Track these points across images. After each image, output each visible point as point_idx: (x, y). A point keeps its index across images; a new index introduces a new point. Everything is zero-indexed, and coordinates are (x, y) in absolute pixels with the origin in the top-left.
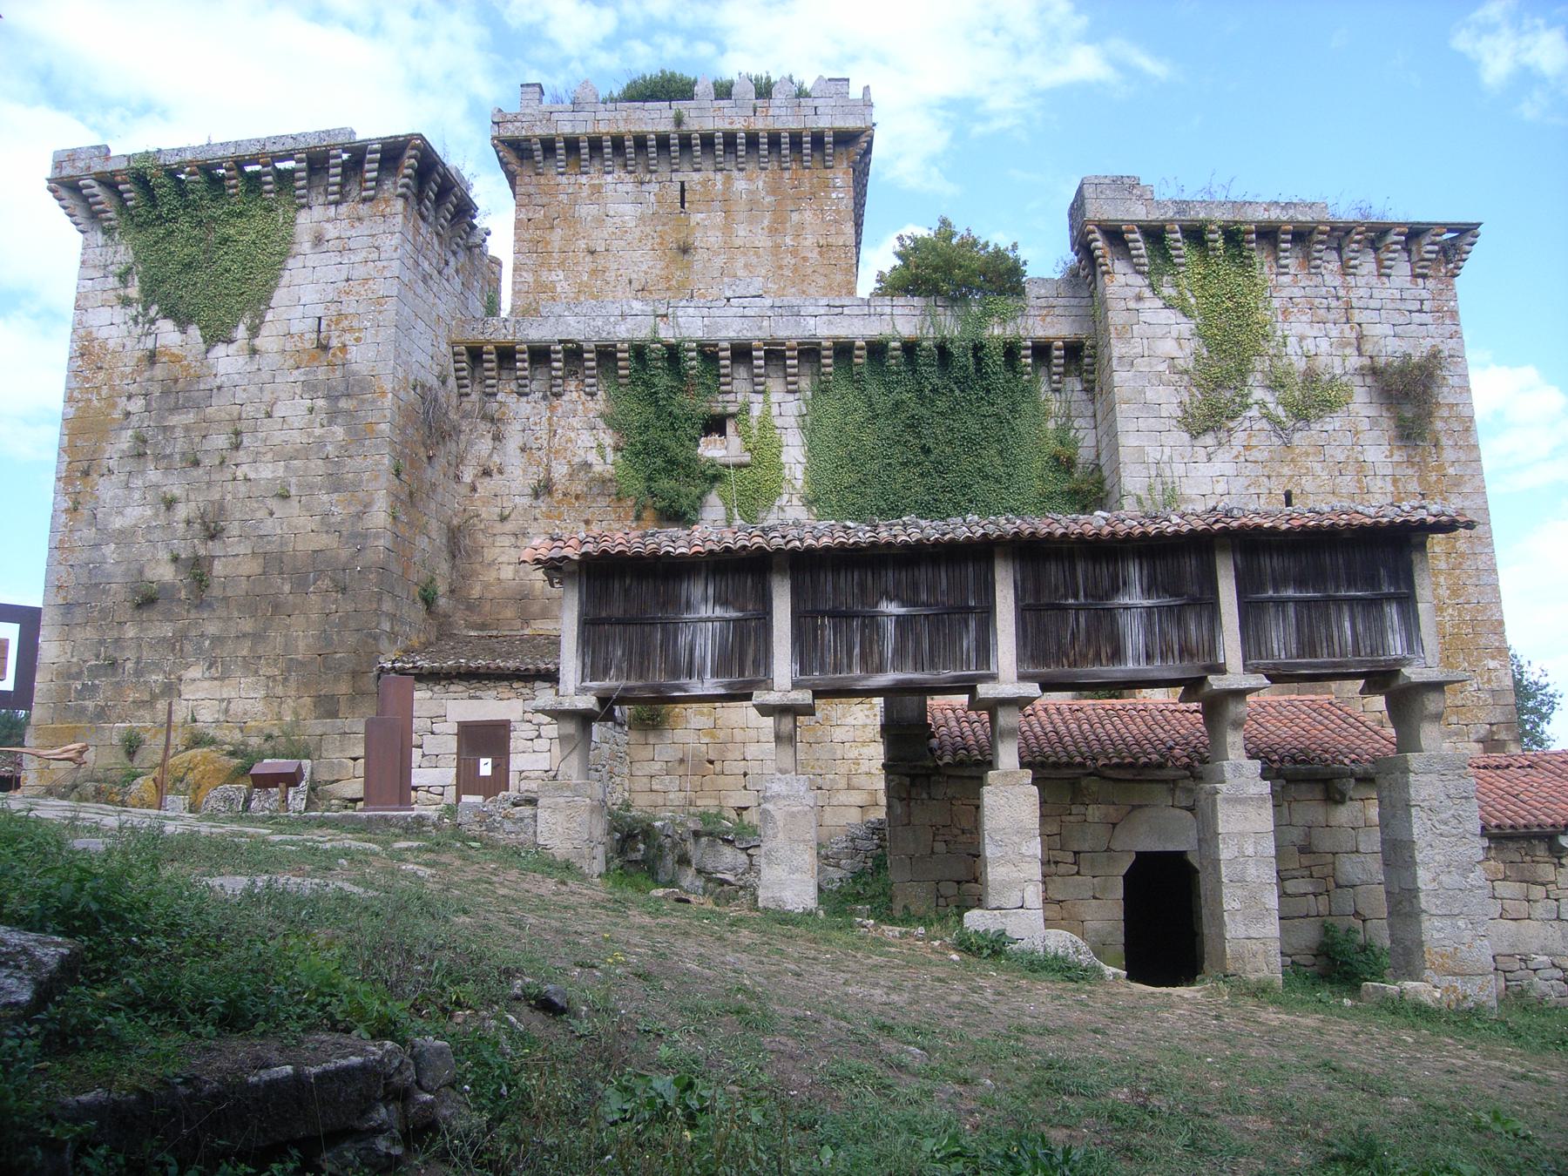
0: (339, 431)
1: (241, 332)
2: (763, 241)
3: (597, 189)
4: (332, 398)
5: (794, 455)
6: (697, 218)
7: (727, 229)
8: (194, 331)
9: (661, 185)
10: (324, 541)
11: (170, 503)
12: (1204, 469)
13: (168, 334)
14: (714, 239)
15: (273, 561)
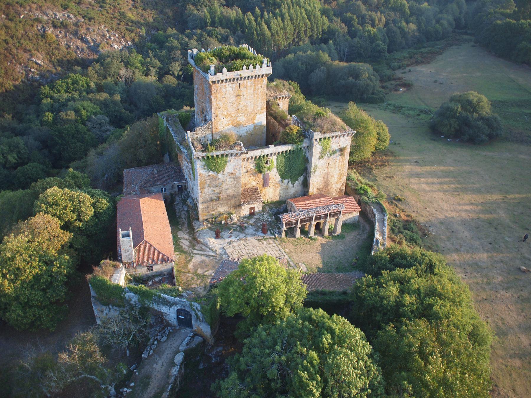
0: (235, 182)
1: (222, 172)
2: (252, 92)
3: (225, 86)
4: (234, 178)
5: (275, 163)
6: (242, 89)
7: (247, 91)
8: (215, 172)
9: (236, 84)
10: (235, 193)
11: (214, 191)
12: (320, 162)
13: (212, 173)
14: (244, 93)
15: (228, 196)
